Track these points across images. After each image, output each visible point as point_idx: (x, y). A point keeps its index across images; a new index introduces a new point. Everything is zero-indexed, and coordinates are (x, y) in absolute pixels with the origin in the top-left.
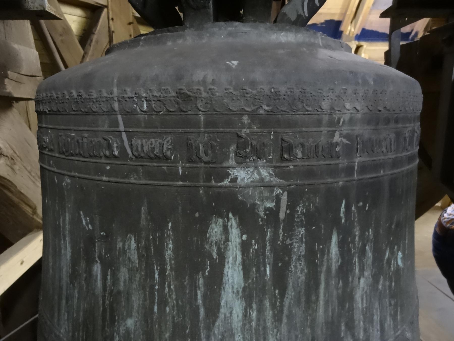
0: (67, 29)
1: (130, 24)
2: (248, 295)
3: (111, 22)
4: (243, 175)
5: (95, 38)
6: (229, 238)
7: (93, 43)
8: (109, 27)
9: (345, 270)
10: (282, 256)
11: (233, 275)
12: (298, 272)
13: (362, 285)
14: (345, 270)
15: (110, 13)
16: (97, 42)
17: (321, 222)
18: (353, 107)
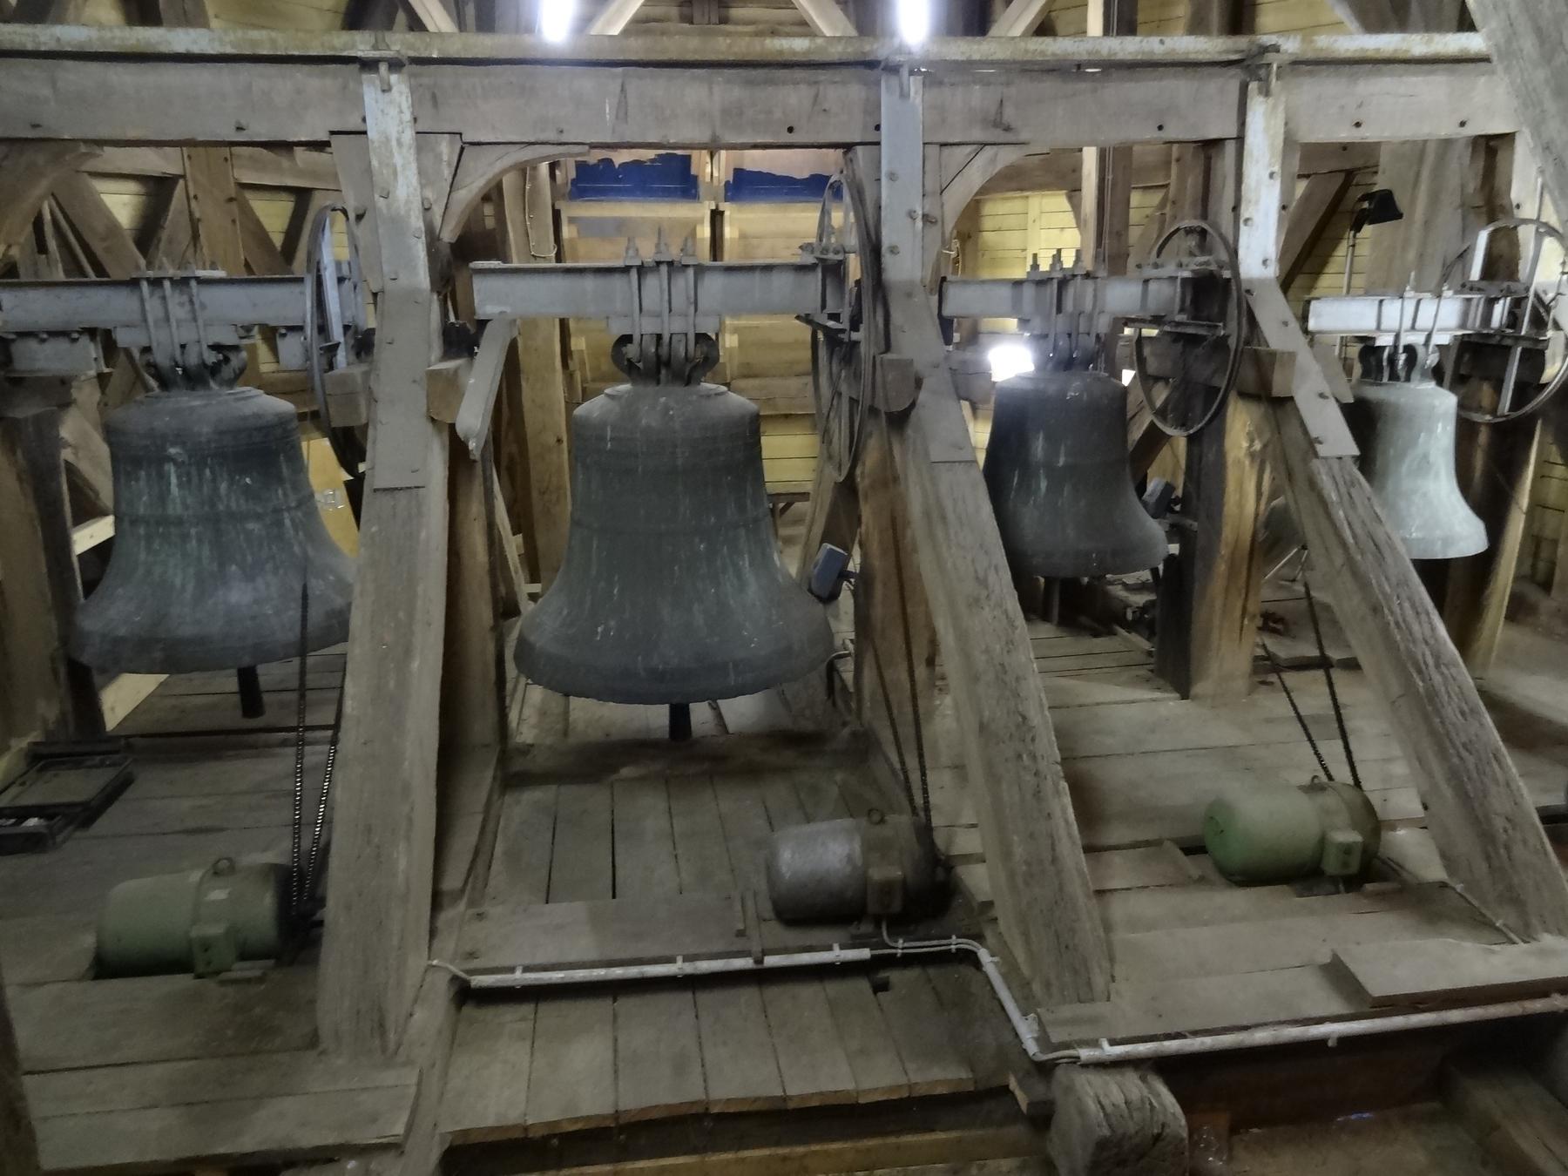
0: (113, 226)
1: (231, 200)
2: (180, 485)
3: (193, 203)
4: (172, 451)
5: (164, 235)
6: (171, 469)
7: (162, 245)
8: (191, 214)
9: (214, 480)
10: (188, 474)
11: (174, 480)
12: (195, 480)
13: (223, 487)
14: (214, 480)
15: (190, 184)
16: (170, 241)
17: (201, 464)
18: (206, 429)
